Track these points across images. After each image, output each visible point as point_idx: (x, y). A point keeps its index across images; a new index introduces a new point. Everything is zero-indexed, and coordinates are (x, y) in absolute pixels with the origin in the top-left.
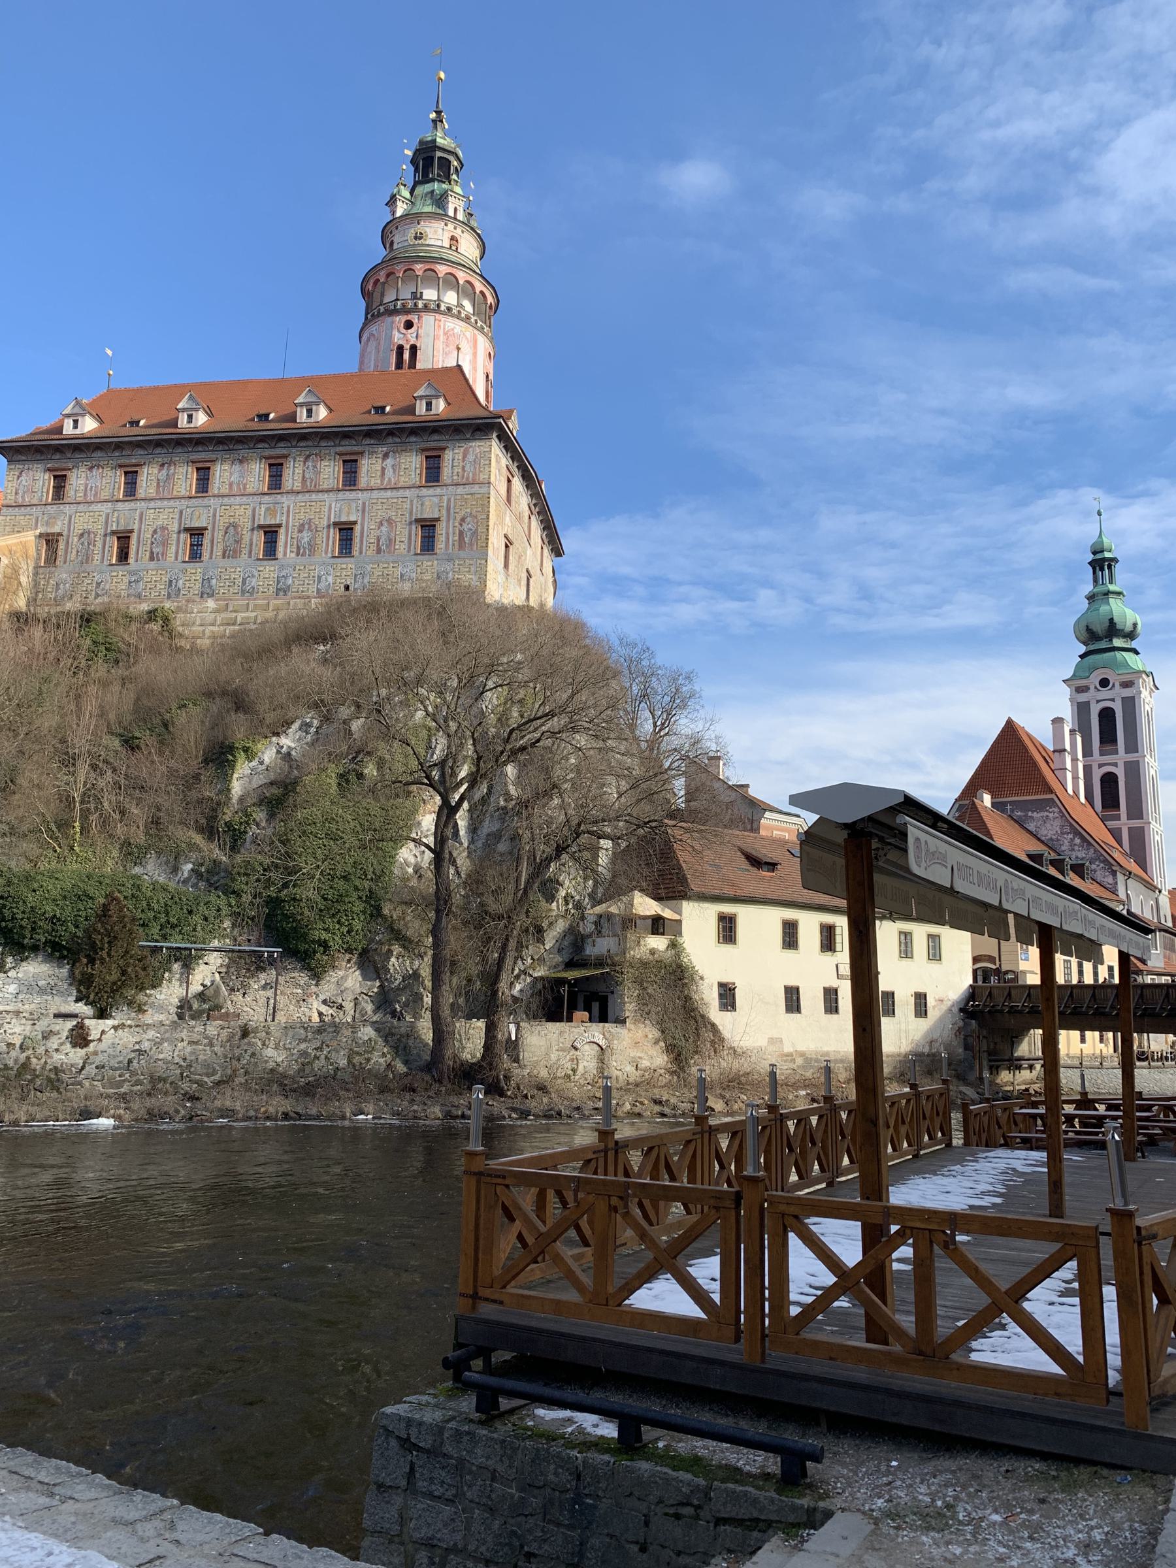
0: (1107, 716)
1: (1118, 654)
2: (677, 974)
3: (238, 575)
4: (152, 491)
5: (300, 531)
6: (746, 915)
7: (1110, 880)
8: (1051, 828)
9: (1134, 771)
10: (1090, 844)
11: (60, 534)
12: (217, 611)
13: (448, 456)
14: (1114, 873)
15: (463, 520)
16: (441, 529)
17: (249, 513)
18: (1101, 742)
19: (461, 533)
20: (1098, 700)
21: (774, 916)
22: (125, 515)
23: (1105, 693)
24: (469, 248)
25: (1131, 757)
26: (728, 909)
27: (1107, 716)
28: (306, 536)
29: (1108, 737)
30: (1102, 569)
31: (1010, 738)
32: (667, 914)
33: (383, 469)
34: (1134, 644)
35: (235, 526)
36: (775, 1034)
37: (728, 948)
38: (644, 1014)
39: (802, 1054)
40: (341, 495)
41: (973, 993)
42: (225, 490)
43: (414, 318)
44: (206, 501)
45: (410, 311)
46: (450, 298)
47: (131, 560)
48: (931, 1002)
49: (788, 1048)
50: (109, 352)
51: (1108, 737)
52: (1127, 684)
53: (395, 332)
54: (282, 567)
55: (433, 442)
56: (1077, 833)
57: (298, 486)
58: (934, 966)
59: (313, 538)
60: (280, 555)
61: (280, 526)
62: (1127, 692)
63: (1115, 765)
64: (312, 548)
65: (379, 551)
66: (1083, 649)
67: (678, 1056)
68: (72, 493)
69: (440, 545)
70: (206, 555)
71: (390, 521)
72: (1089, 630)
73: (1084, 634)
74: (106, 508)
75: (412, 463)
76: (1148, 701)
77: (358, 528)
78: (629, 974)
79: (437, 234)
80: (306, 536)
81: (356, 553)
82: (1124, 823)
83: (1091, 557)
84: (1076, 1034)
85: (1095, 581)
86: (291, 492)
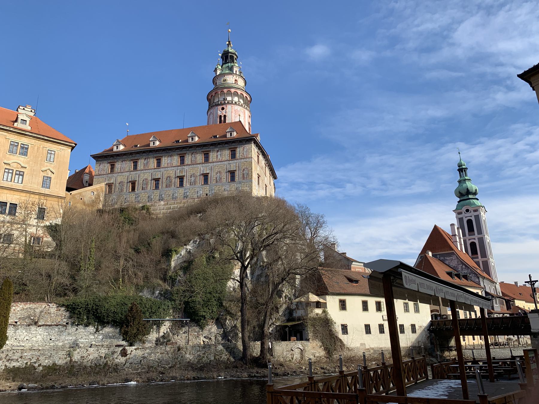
0: (470, 222)
1: (471, 201)
2: (326, 322)
3: (171, 193)
4: (142, 167)
5: (191, 177)
6: (349, 300)
7: (477, 280)
8: (454, 263)
9: (482, 241)
10: (468, 268)
11: (113, 183)
12: (164, 205)
13: (238, 150)
14: (478, 278)
15: (244, 170)
16: (237, 173)
17: (174, 172)
18: (469, 231)
19: (243, 174)
20: (466, 217)
21: (359, 300)
22: (134, 175)
23: (468, 214)
24: (241, 83)
25: (480, 236)
26: (342, 298)
27: (470, 222)
28: (193, 179)
29: (471, 229)
30: (462, 172)
31: (436, 233)
32: (321, 300)
33: (217, 156)
34: (476, 197)
35: (170, 177)
36: (362, 342)
37: (343, 312)
38: (316, 337)
39: (373, 349)
40: (203, 165)
41: (432, 323)
42: (166, 166)
44: (160, 170)
45: (223, 104)
46: (236, 99)
47: (136, 190)
48: (417, 327)
49: (367, 347)
50: (127, 124)
51: (471, 229)
52: (475, 211)
53: (219, 112)
54: (185, 189)
56: (463, 264)
57: (190, 163)
58: (417, 314)
59: (195, 179)
60: (184, 185)
61: (184, 176)
62: (476, 214)
63: (475, 239)
64: (195, 183)
65: (217, 182)
66: (458, 199)
67: (329, 352)
68: (116, 170)
69: (237, 179)
70: (160, 187)
71: (220, 172)
72: (460, 193)
73: (459, 195)
74: (127, 174)
75: (226, 153)
76: (484, 216)
77: (209, 175)
78: (309, 323)
79: (230, 79)
80: (193, 179)
81: (209, 183)
82: (480, 259)
83: (458, 168)
84: (471, 337)
85: (460, 176)
86: (188, 165)
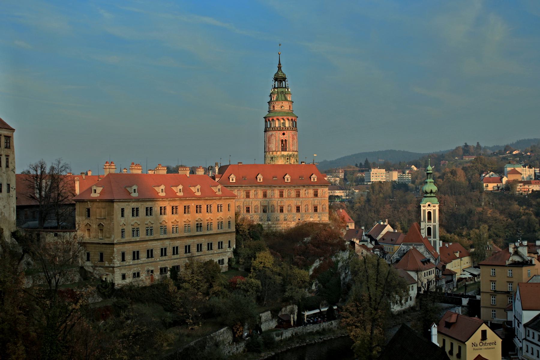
0: (429, 213)
16: (318, 207)
23: (429, 208)
27: (429, 213)
43: (285, 132)
55: (316, 188)
62: (434, 208)
69: (318, 210)
74: (243, 200)
80: (290, 208)
